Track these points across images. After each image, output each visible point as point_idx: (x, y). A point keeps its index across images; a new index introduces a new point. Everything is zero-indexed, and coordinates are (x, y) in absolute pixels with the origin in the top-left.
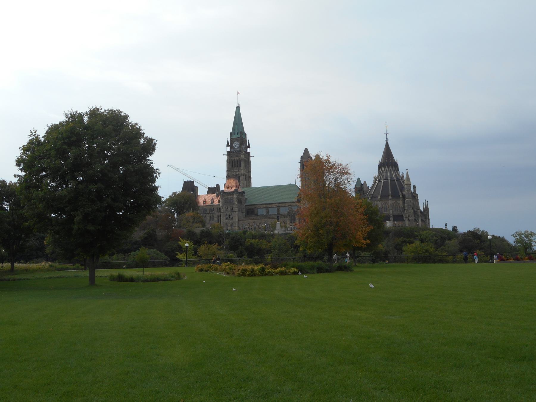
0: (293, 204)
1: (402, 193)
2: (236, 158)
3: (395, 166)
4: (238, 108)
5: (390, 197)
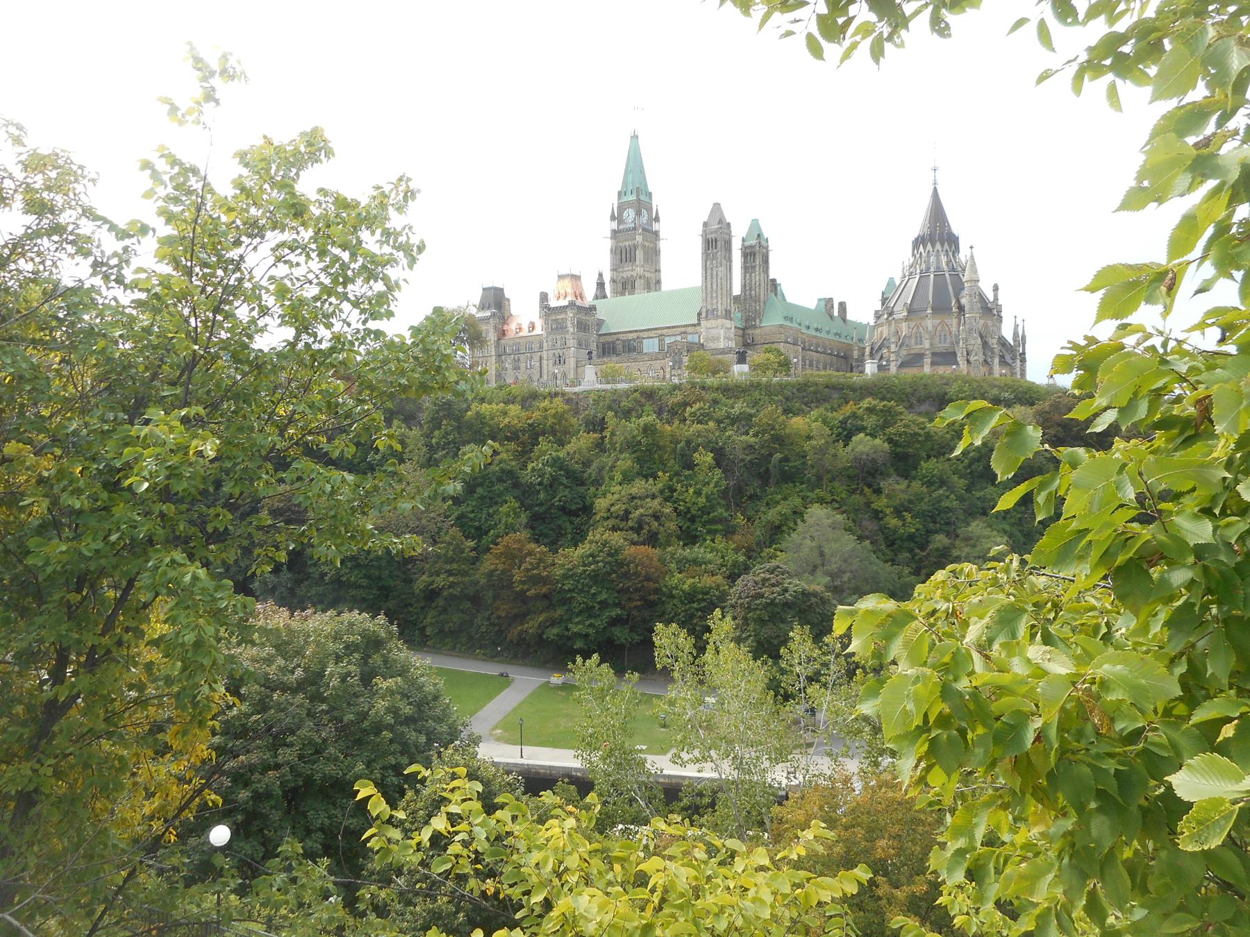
0: (690, 330)
1: (958, 301)
2: (627, 244)
3: (952, 242)
4: (635, 137)
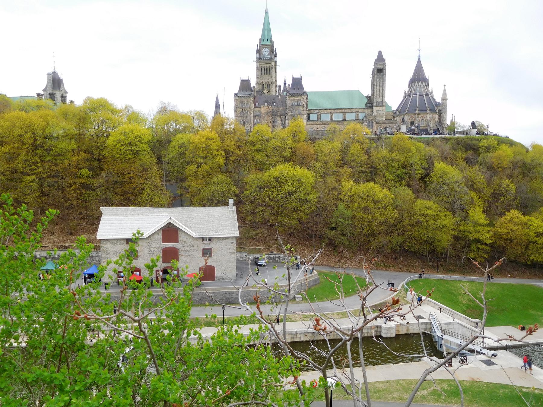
0: (360, 110)
2: (265, 65)
4: (267, 13)
5: (428, 111)
